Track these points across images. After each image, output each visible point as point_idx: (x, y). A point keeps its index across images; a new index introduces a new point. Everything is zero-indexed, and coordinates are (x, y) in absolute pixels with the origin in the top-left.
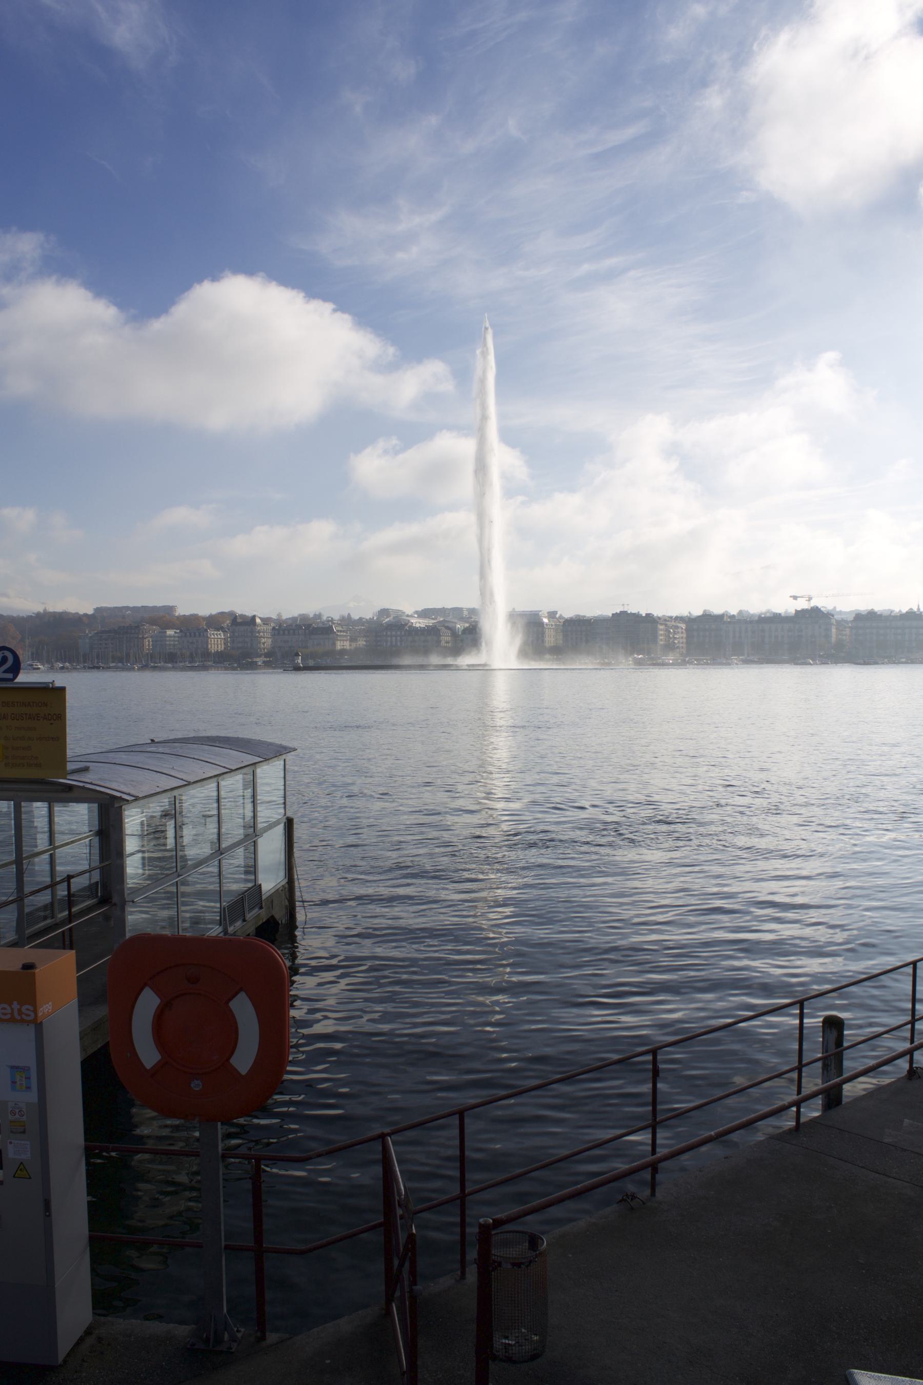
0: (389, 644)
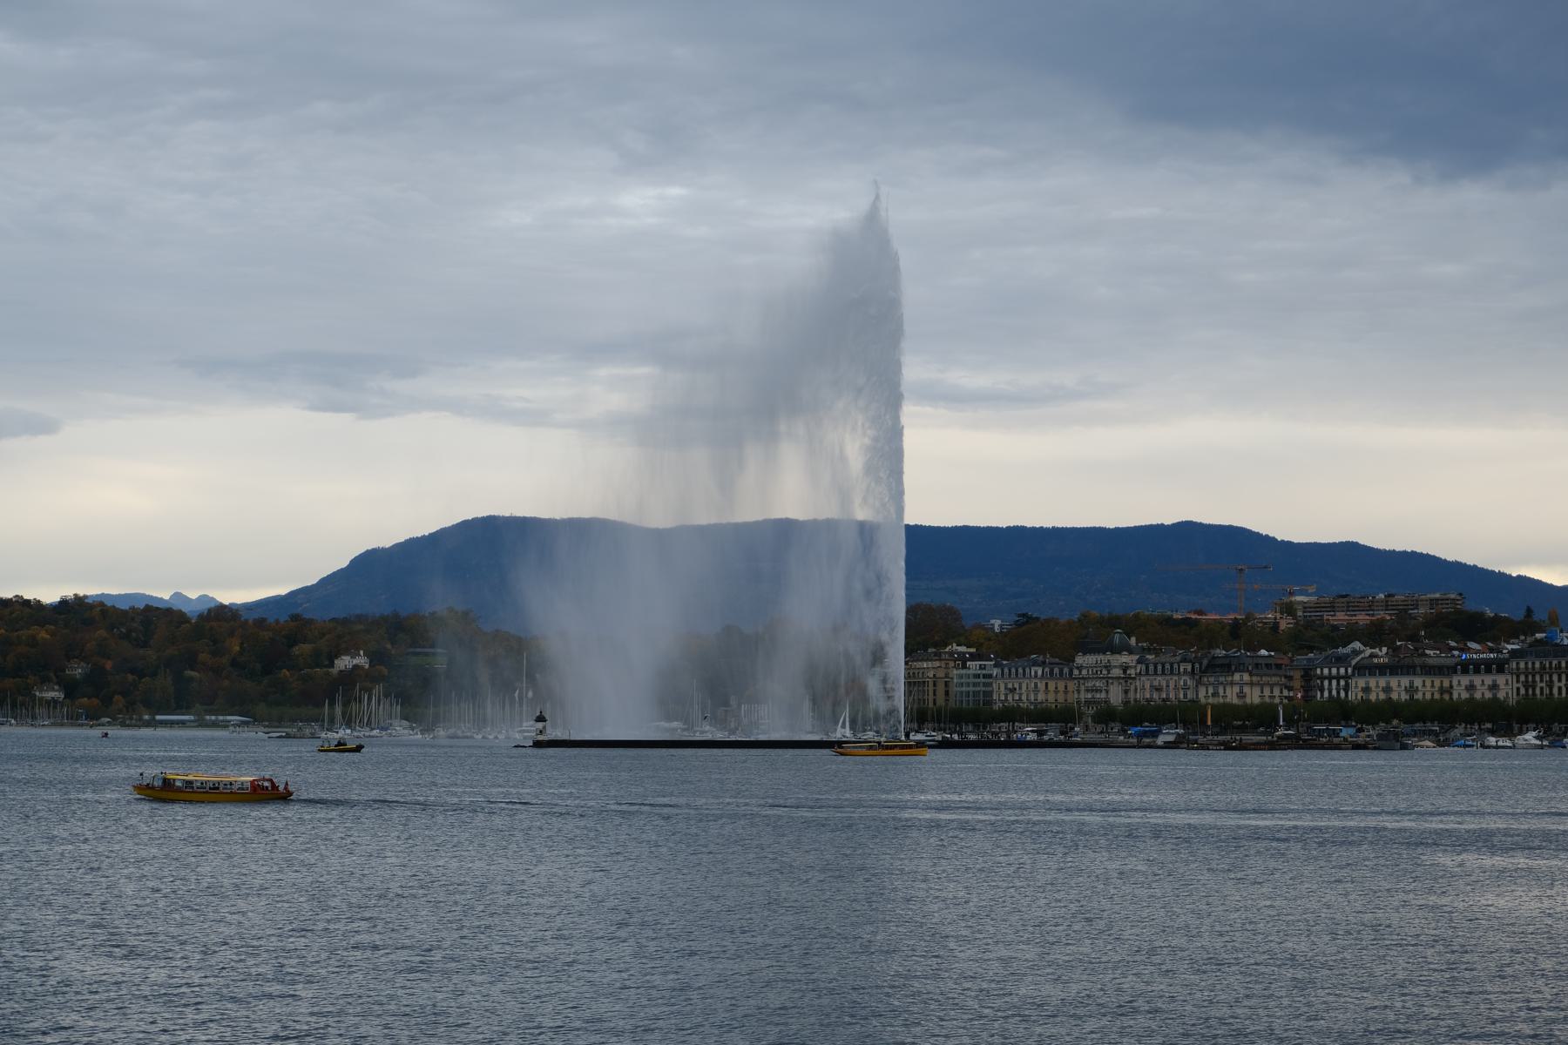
0: (1326, 694)
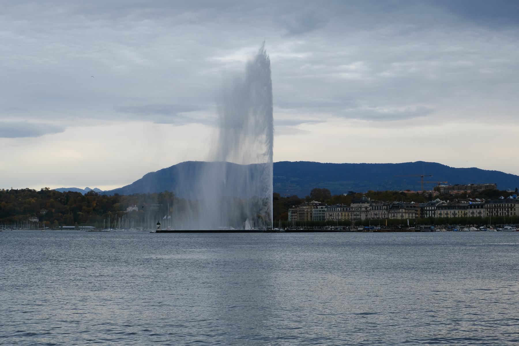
0: (428, 216)
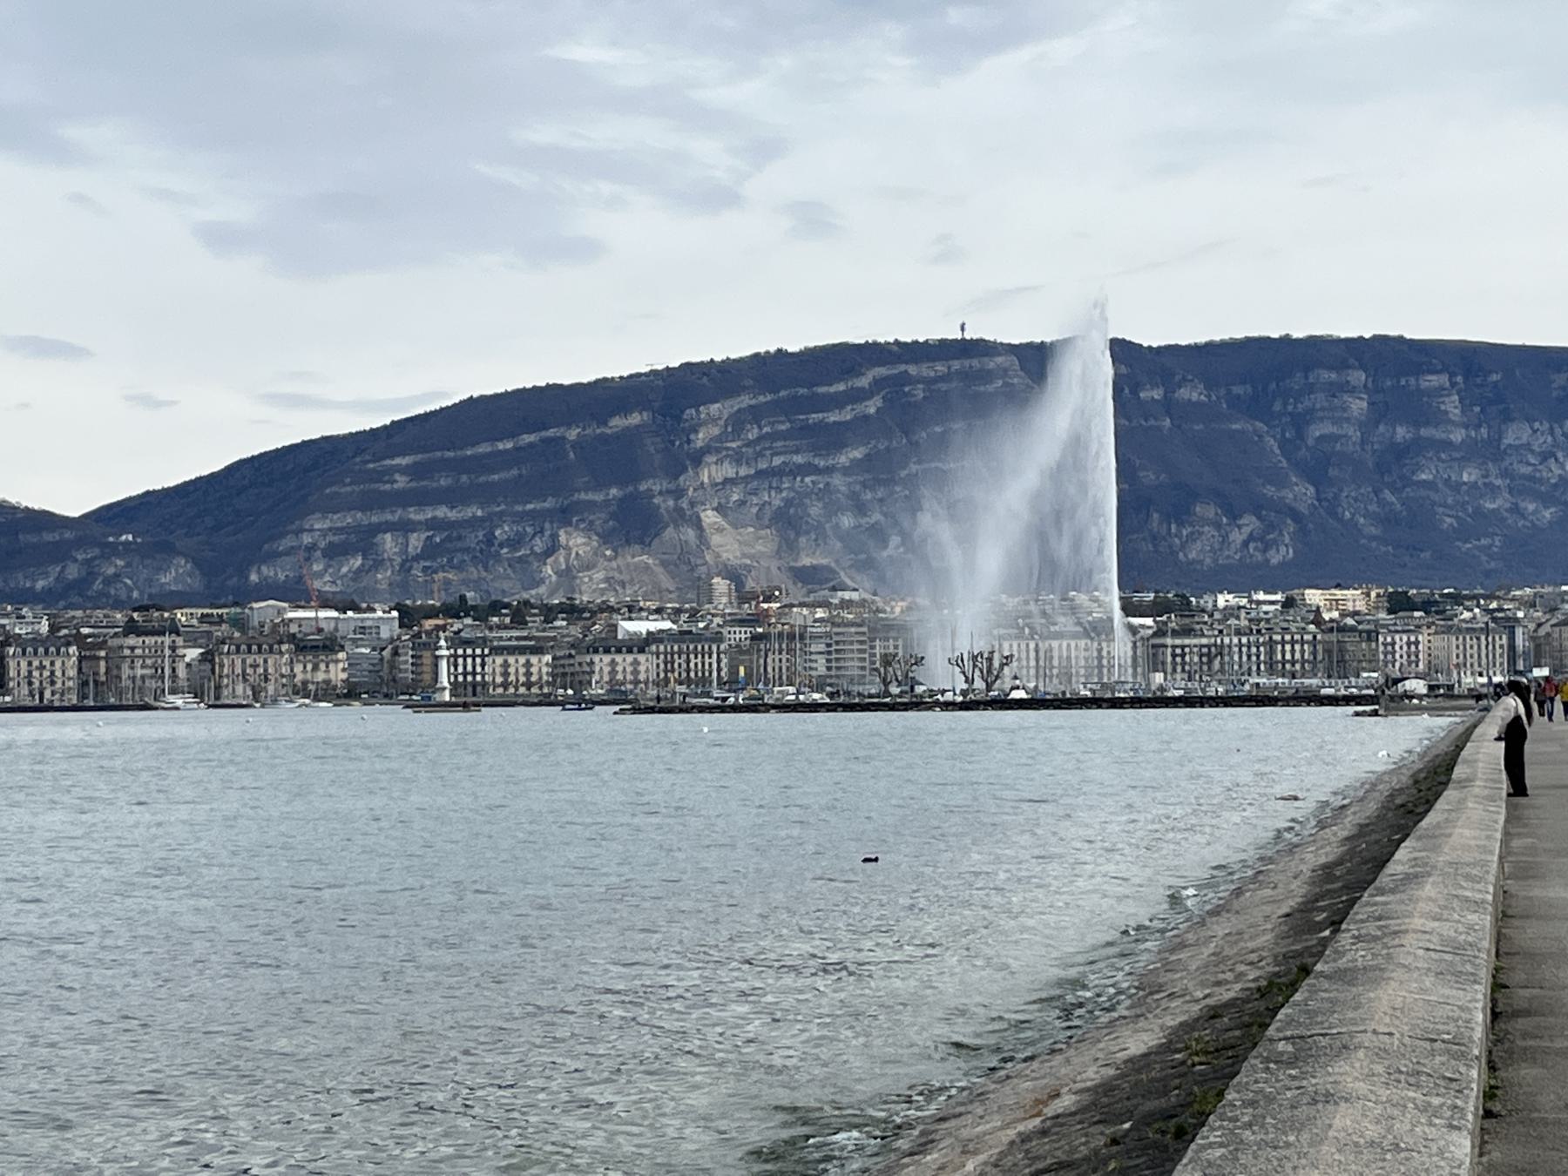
0: (460, 669)
